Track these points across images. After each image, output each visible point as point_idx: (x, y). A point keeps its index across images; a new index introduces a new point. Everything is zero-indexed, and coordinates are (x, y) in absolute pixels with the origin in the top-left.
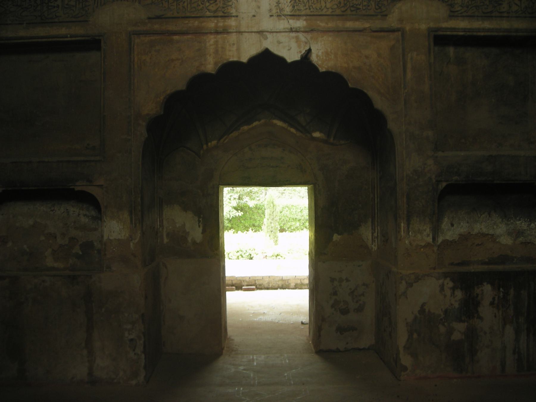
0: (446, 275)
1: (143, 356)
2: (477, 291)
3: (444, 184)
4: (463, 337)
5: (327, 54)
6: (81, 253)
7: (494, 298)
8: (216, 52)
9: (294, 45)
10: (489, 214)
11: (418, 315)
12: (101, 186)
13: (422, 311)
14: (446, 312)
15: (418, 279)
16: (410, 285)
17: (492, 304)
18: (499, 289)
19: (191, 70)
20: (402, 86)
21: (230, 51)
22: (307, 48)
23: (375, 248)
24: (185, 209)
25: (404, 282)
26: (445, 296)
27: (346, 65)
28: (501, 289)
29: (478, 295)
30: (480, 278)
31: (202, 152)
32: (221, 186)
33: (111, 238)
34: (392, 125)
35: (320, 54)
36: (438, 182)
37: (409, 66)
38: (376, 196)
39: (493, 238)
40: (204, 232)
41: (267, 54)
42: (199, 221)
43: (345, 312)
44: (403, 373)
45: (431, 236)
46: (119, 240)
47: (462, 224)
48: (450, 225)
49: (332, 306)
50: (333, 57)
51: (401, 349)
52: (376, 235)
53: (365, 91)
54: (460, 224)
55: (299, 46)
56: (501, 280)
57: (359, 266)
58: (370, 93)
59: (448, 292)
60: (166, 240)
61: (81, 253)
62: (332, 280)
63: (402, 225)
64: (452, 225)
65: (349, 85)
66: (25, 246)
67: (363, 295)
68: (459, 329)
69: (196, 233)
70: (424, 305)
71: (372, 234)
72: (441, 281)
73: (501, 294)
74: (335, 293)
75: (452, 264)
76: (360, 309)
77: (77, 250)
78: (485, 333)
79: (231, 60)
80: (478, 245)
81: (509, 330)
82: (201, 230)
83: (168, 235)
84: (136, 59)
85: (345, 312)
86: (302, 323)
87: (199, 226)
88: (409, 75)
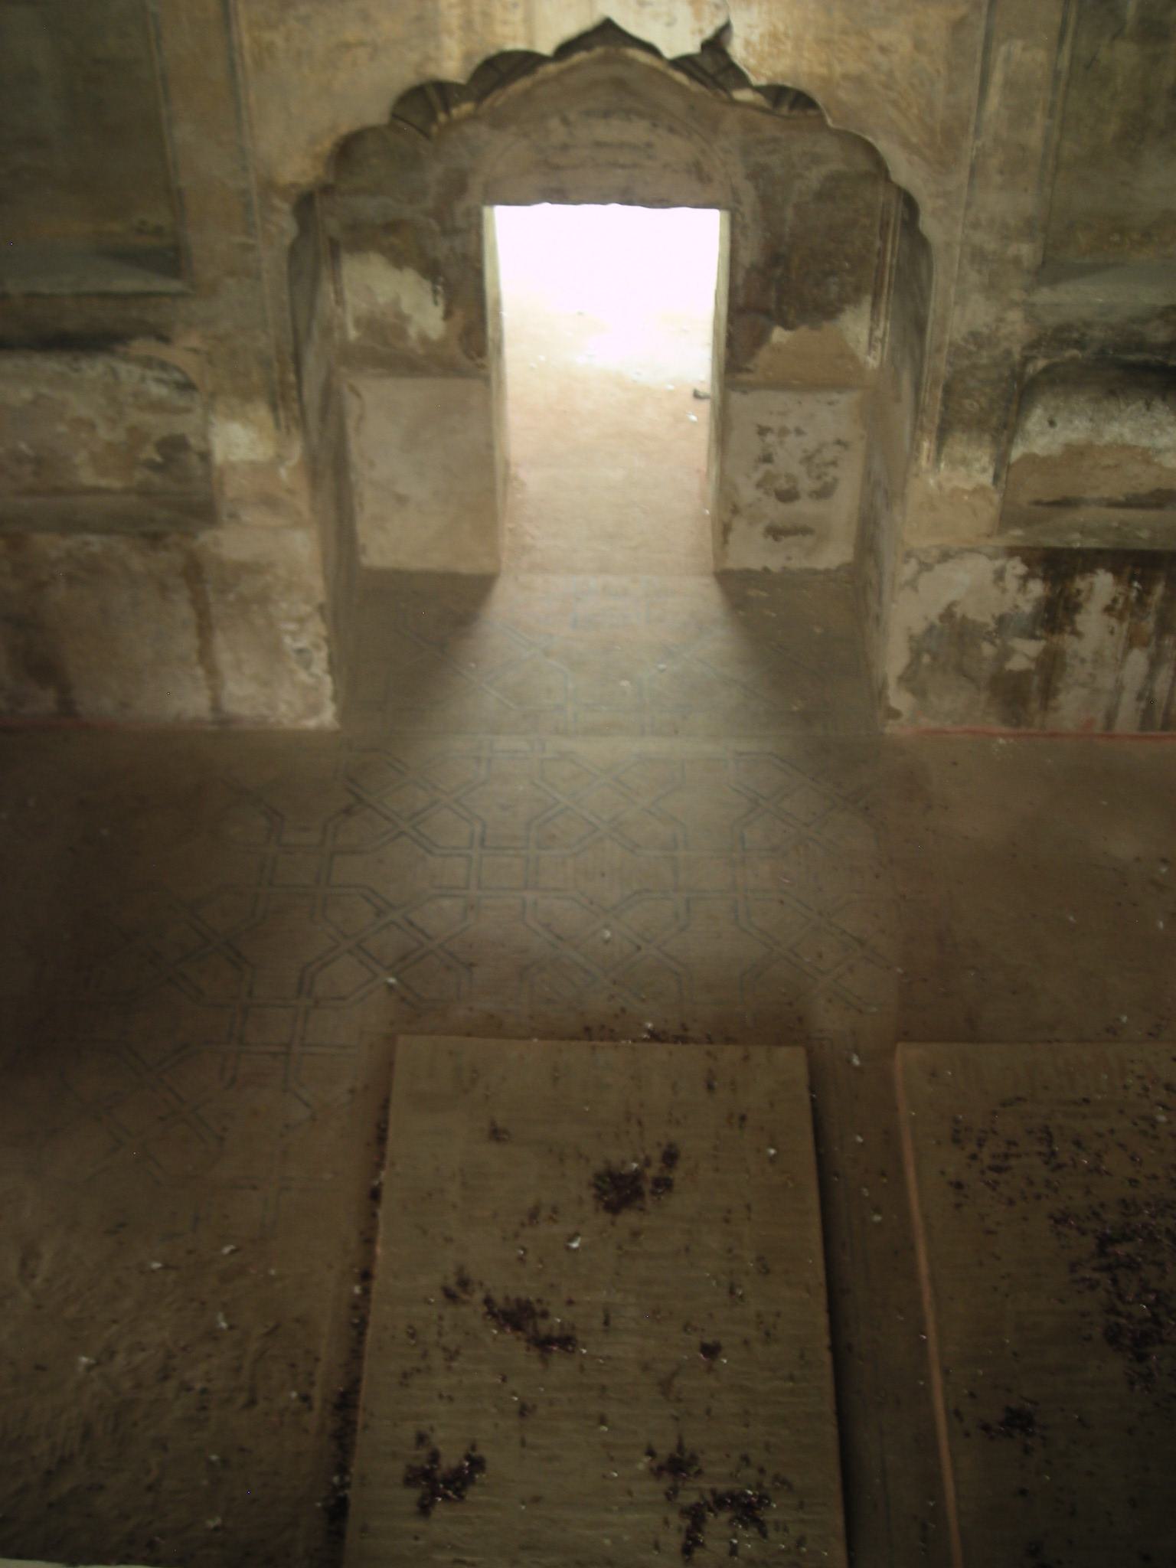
0: (1012, 552)
1: (328, 679)
2: (1080, 584)
3: (1041, 363)
4: (1033, 666)
5: (774, 37)
6: (158, 459)
7: (1115, 600)
8: (468, 25)
9: (683, 12)
10: (1148, 406)
11: (937, 622)
12: (195, 351)
13: (948, 614)
14: (1001, 621)
15: (946, 556)
16: (925, 567)
17: (1109, 610)
18: (1130, 586)
19: (404, 77)
20: (972, 129)
21: (505, 23)
22: (720, 22)
23: (872, 362)
24: (398, 260)
25: (913, 563)
26: (1004, 591)
27: (823, 71)
28: (1136, 584)
29: (1079, 592)
30: (1089, 560)
31: (434, 129)
32: (486, 210)
33: (233, 458)
34: (928, 225)
35: (755, 38)
36: (1026, 360)
37: (997, 77)
38: (889, 246)
39: (1146, 457)
40: (448, 315)
41: (607, 32)
42: (435, 292)
43: (787, 496)
44: (891, 722)
45: (991, 471)
46: (252, 463)
47: (1077, 422)
48: (1046, 423)
49: (759, 485)
50: (789, 46)
51: (892, 682)
52: (879, 333)
53: (870, 139)
54: (1071, 422)
55: (698, 15)
56: (1136, 564)
57: (830, 403)
58: (883, 145)
59: (1011, 584)
60: (353, 334)
61: (158, 459)
62: (763, 431)
63: (926, 445)
64: (1052, 423)
65: (829, 121)
66: (23, 446)
67: (834, 463)
68: (1025, 653)
69: (427, 318)
70: (951, 606)
71: (871, 331)
72: (999, 563)
73: (1134, 594)
74: (767, 459)
75: (1038, 503)
76: (824, 493)
77: (150, 453)
78: (1083, 661)
79: (510, 46)
80: (1109, 467)
81: (1138, 659)
82: (438, 311)
83: (358, 323)
84: (246, 41)
85: (787, 496)
86: (697, 395)
87: (436, 303)
88: (994, 100)
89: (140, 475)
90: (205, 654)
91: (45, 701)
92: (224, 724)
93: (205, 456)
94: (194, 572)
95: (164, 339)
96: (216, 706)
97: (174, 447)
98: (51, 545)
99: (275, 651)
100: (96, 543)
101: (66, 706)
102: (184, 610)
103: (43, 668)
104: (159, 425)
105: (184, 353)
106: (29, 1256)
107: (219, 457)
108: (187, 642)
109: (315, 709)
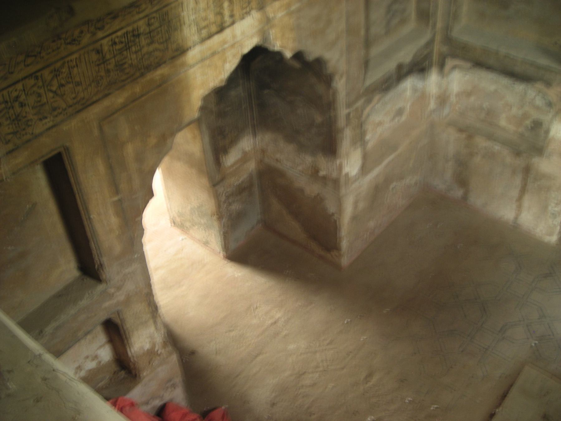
77: (528, 122)
89: (521, 130)
90: (520, 199)
91: (459, 193)
92: (515, 227)
93: (547, 132)
94: (527, 170)
95: (548, 84)
96: (516, 218)
97: (537, 125)
98: (481, 143)
99: (545, 208)
100: (497, 148)
101: (465, 197)
102: (518, 181)
103: (462, 180)
104: (535, 115)
105: (553, 93)
106: (370, 375)
107: (552, 133)
108: (515, 193)
109: (551, 234)
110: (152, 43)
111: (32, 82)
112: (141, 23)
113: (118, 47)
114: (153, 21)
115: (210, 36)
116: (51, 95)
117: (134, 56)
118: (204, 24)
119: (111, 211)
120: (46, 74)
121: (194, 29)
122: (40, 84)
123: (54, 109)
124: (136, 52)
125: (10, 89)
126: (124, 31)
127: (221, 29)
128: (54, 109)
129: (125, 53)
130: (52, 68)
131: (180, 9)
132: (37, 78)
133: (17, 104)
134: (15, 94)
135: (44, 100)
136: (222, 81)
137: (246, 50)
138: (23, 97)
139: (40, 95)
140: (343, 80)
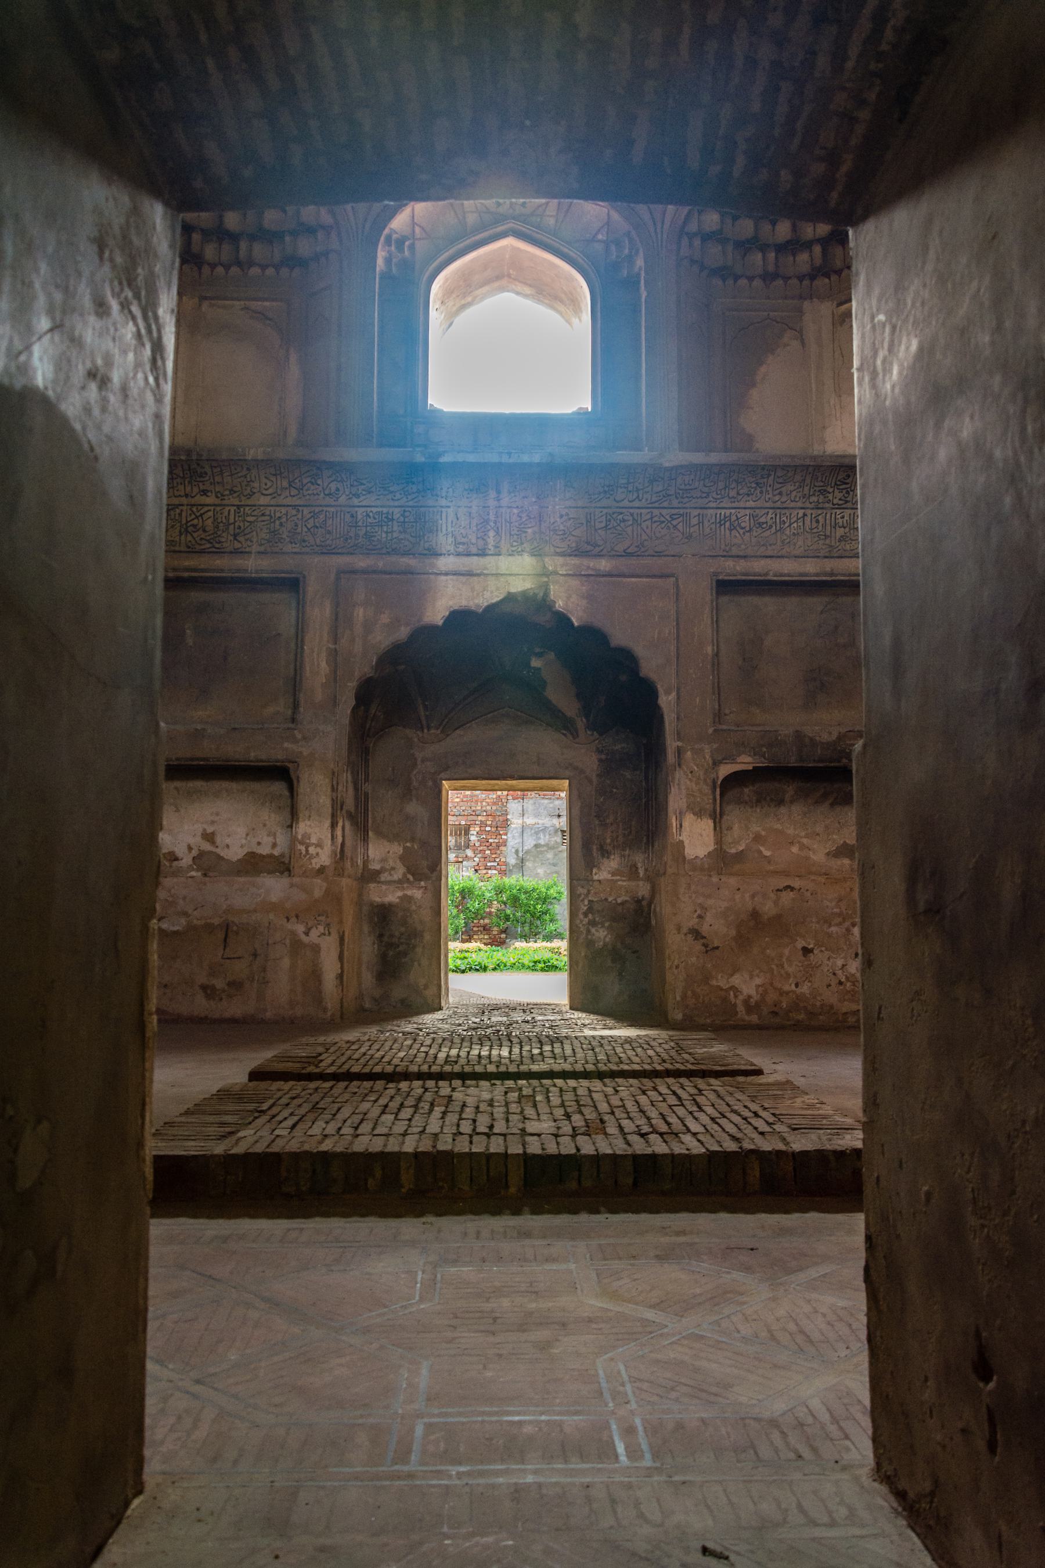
110: (405, 532)
111: (294, 512)
112: (397, 510)
113: (369, 520)
114: (407, 514)
115: (468, 555)
116: (305, 529)
117: (384, 535)
118: (463, 540)
119: (324, 655)
120: (306, 511)
121: (450, 540)
122: (300, 516)
123: (304, 541)
124: (387, 532)
125: (278, 509)
126: (380, 509)
127: (482, 553)
128: (304, 541)
129: (377, 529)
130: (313, 509)
131: (438, 517)
132: (298, 511)
133: (277, 522)
134: (278, 515)
135: (299, 530)
136: (478, 606)
137: (513, 590)
138: (284, 520)
139: (296, 525)
140: (673, 696)
